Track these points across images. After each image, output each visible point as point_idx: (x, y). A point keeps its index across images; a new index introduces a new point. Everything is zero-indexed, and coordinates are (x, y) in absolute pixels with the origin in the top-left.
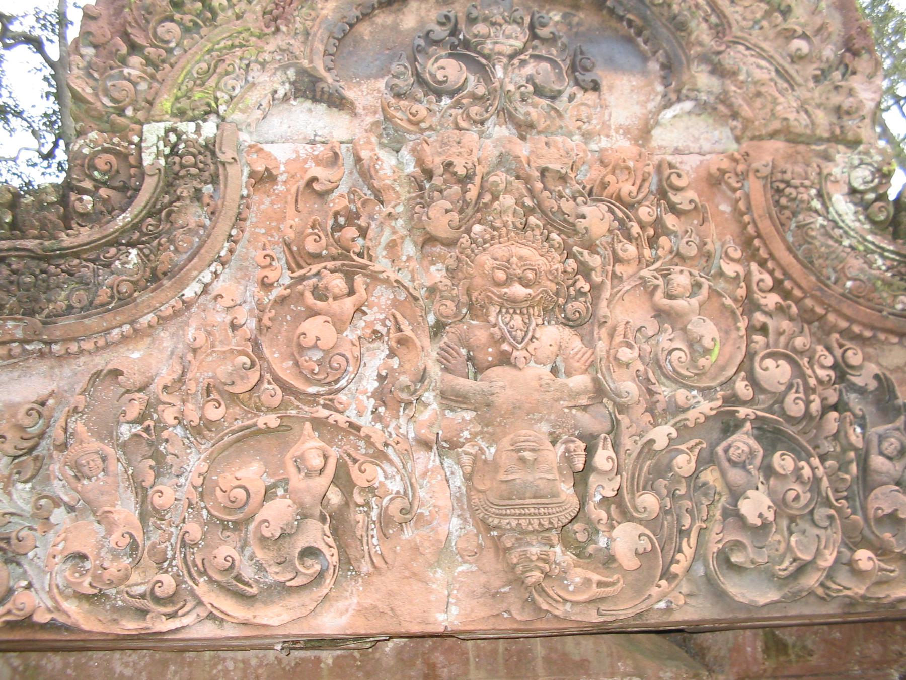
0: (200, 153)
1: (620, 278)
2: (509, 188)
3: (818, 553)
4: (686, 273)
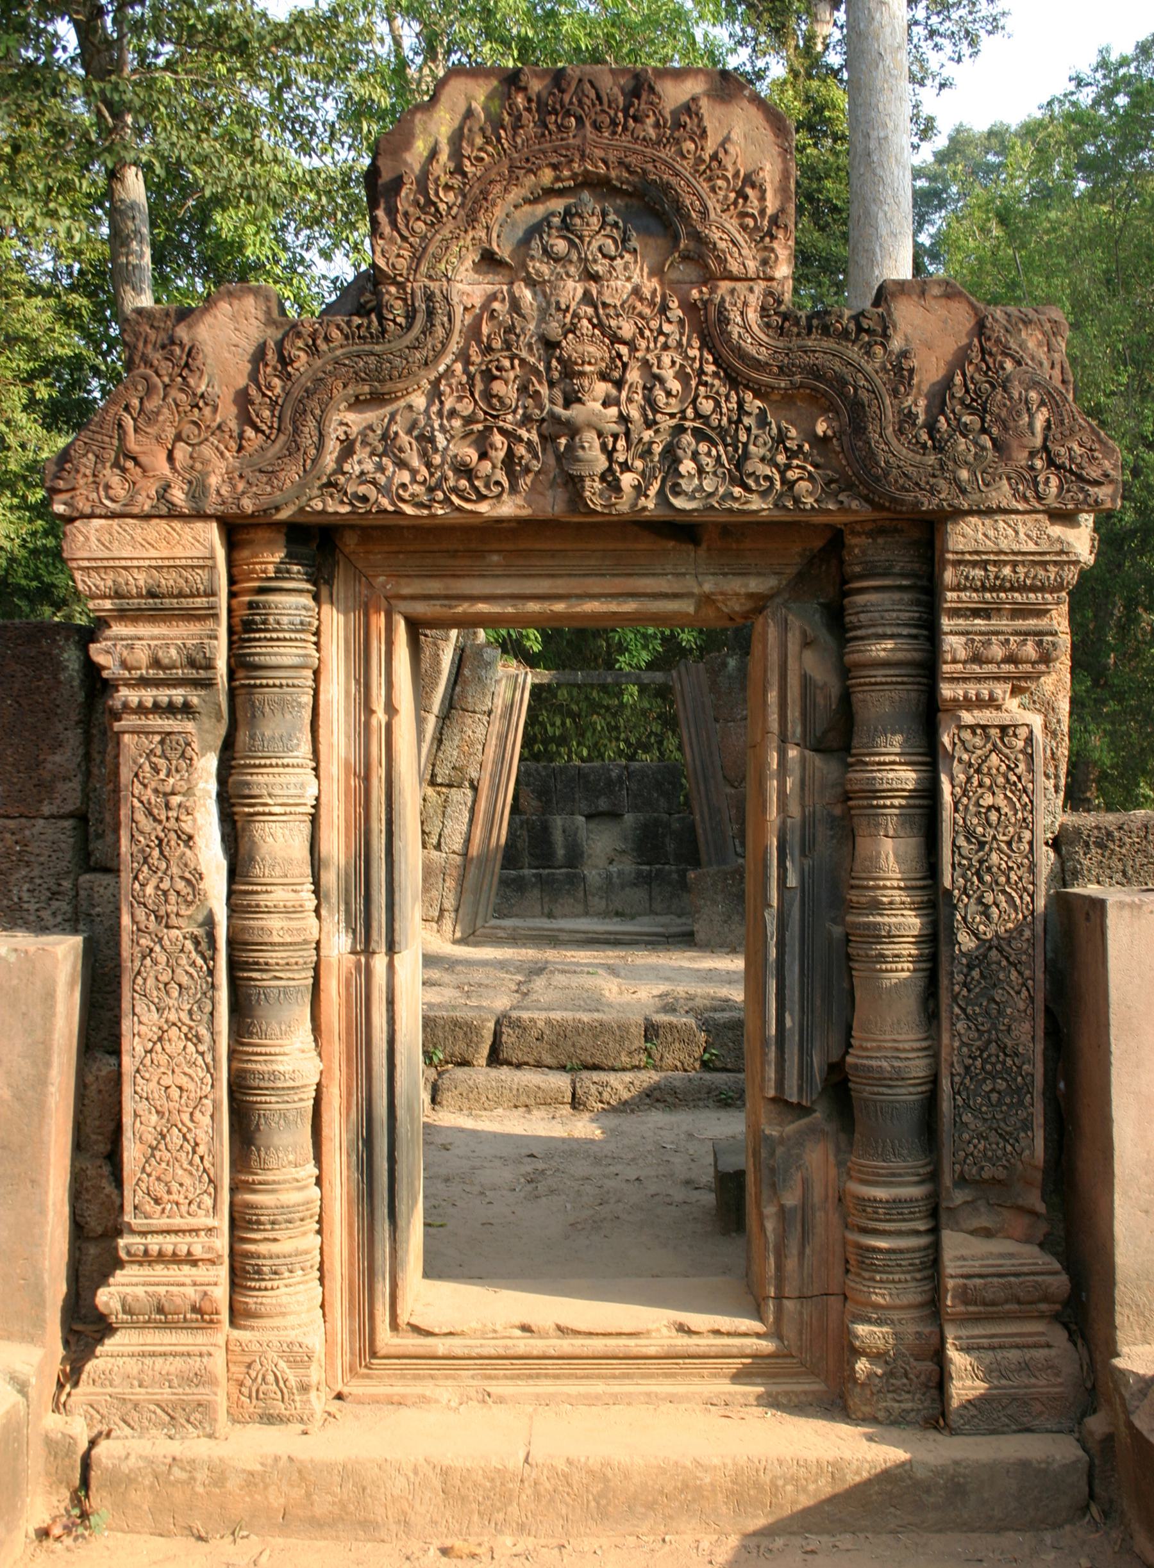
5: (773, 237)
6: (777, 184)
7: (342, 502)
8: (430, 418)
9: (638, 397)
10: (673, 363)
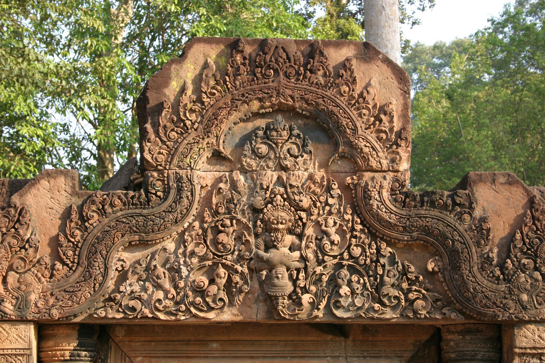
3: (364, 304)
5: (398, 146)
6: (400, 113)
7: (118, 311)
8: (177, 257)
9: (313, 245)
10: (335, 223)
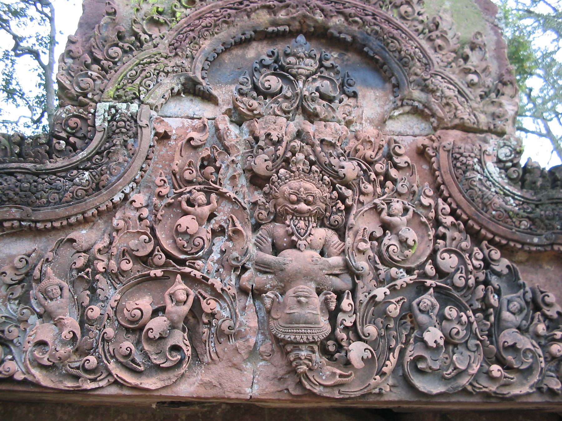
0: (128, 120)
1: (362, 204)
2: (301, 150)
3: (469, 365)
4: (400, 203)
10: (406, 210)
